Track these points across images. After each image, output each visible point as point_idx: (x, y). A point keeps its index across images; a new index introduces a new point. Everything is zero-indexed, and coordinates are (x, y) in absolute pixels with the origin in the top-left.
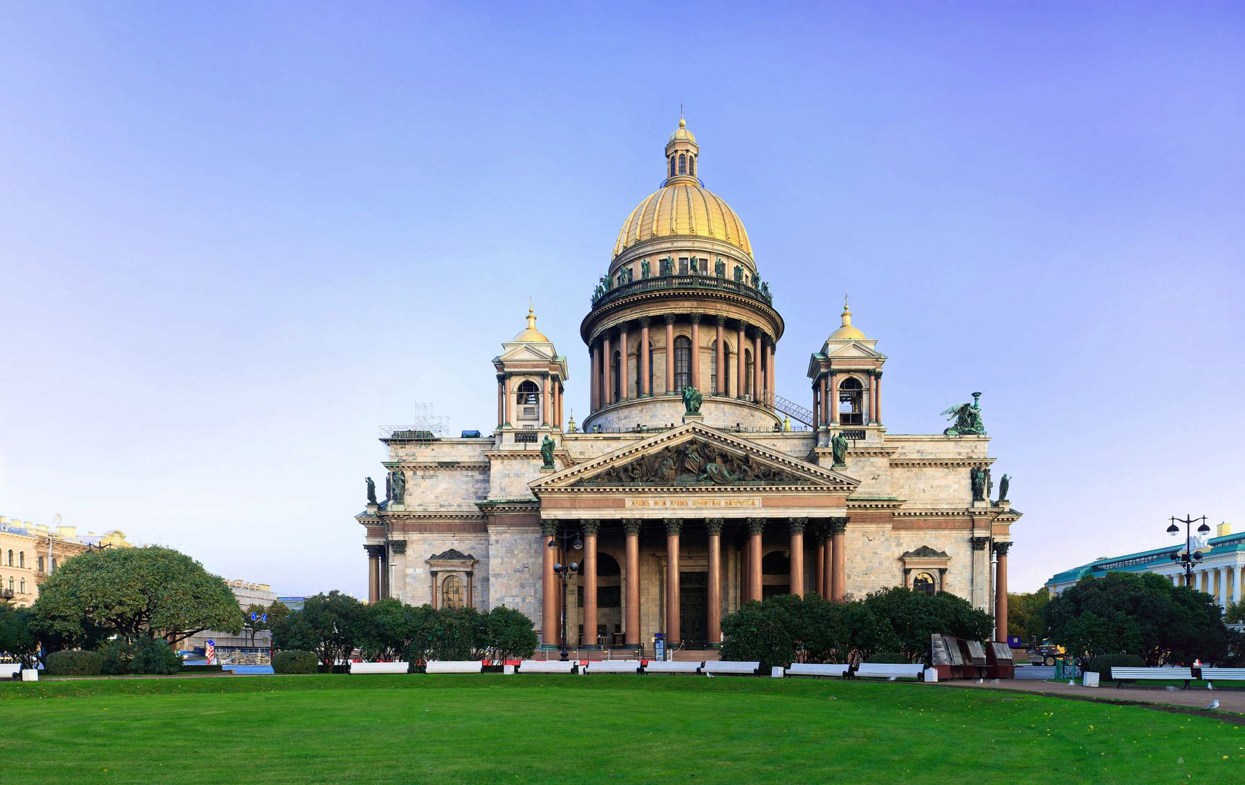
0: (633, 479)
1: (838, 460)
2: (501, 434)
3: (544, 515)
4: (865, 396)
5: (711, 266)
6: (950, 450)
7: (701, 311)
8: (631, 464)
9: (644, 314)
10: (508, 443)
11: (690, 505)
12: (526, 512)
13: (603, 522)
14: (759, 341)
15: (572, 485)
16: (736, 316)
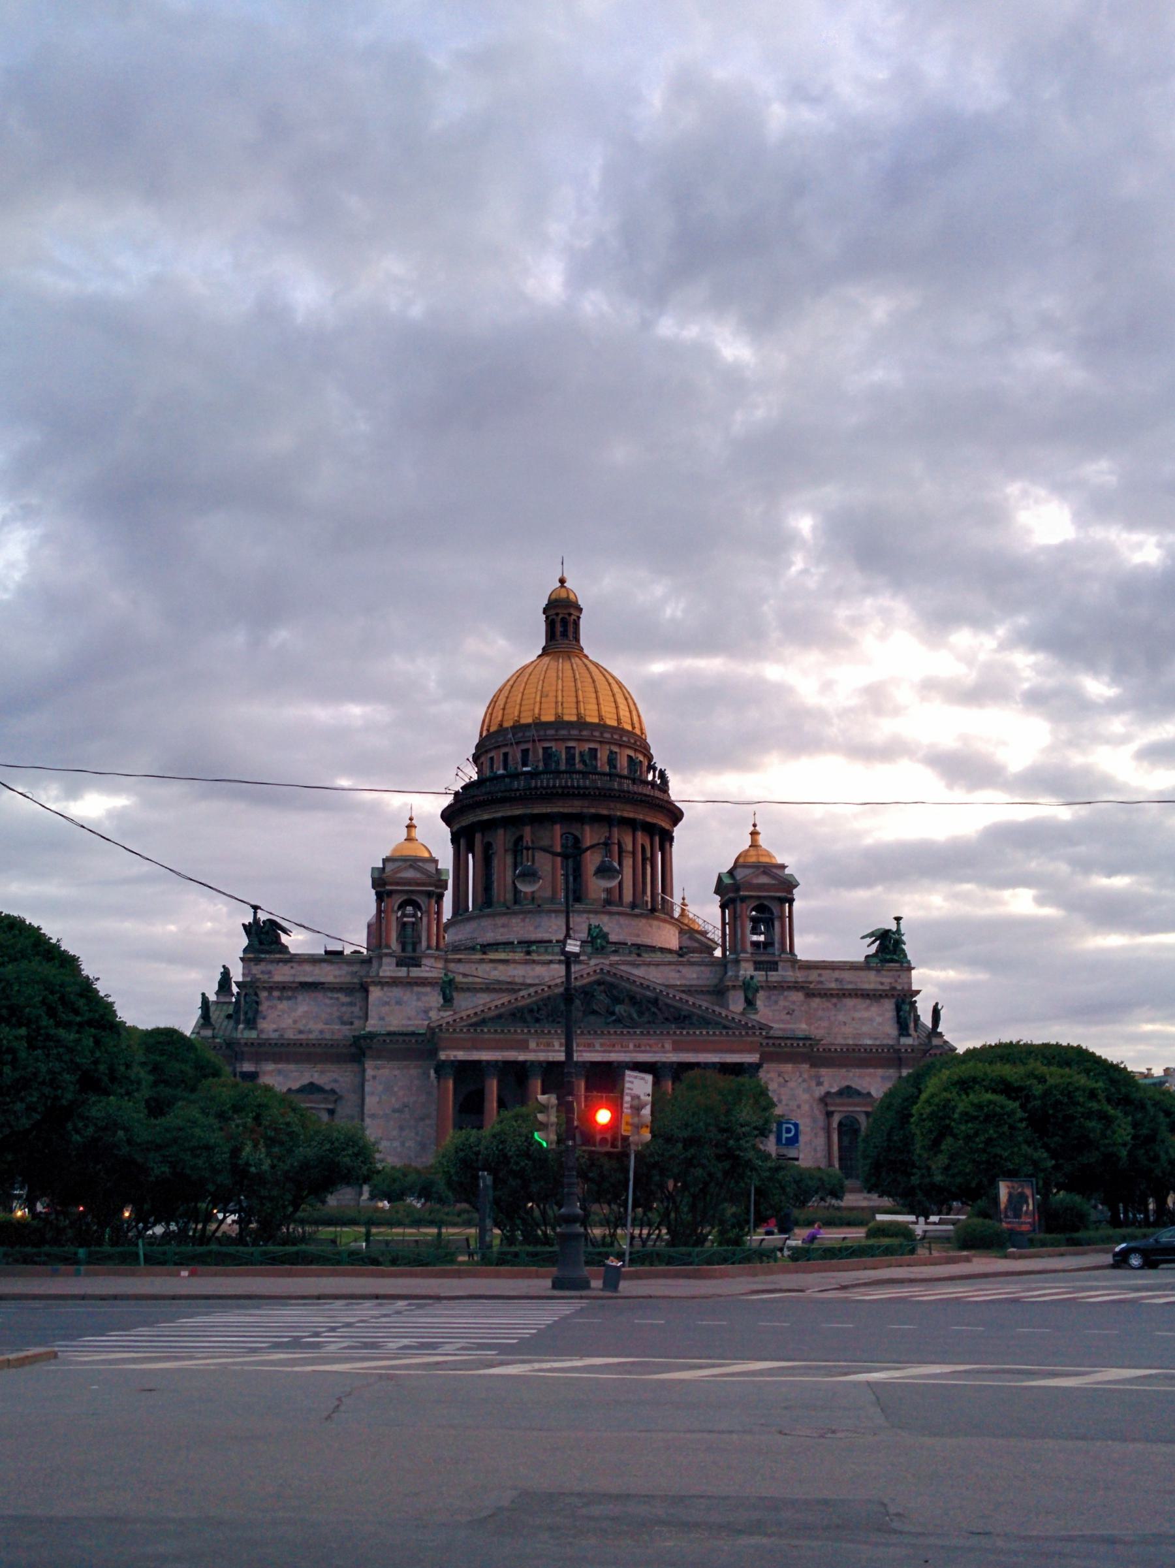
0: (537, 1020)
1: (750, 1003)
2: (380, 957)
3: (443, 1056)
4: (777, 924)
5: (603, 755)
6: (870, 981)
7: (593, 811)
8: (535, 1003)
9: (529, 811)
10: (388, 969)
11: (598, 1047)
12: (418, 1047)
13: (507, 1064)
14: (657, 839)
15: (471, 1025)
16: (631, 815)
